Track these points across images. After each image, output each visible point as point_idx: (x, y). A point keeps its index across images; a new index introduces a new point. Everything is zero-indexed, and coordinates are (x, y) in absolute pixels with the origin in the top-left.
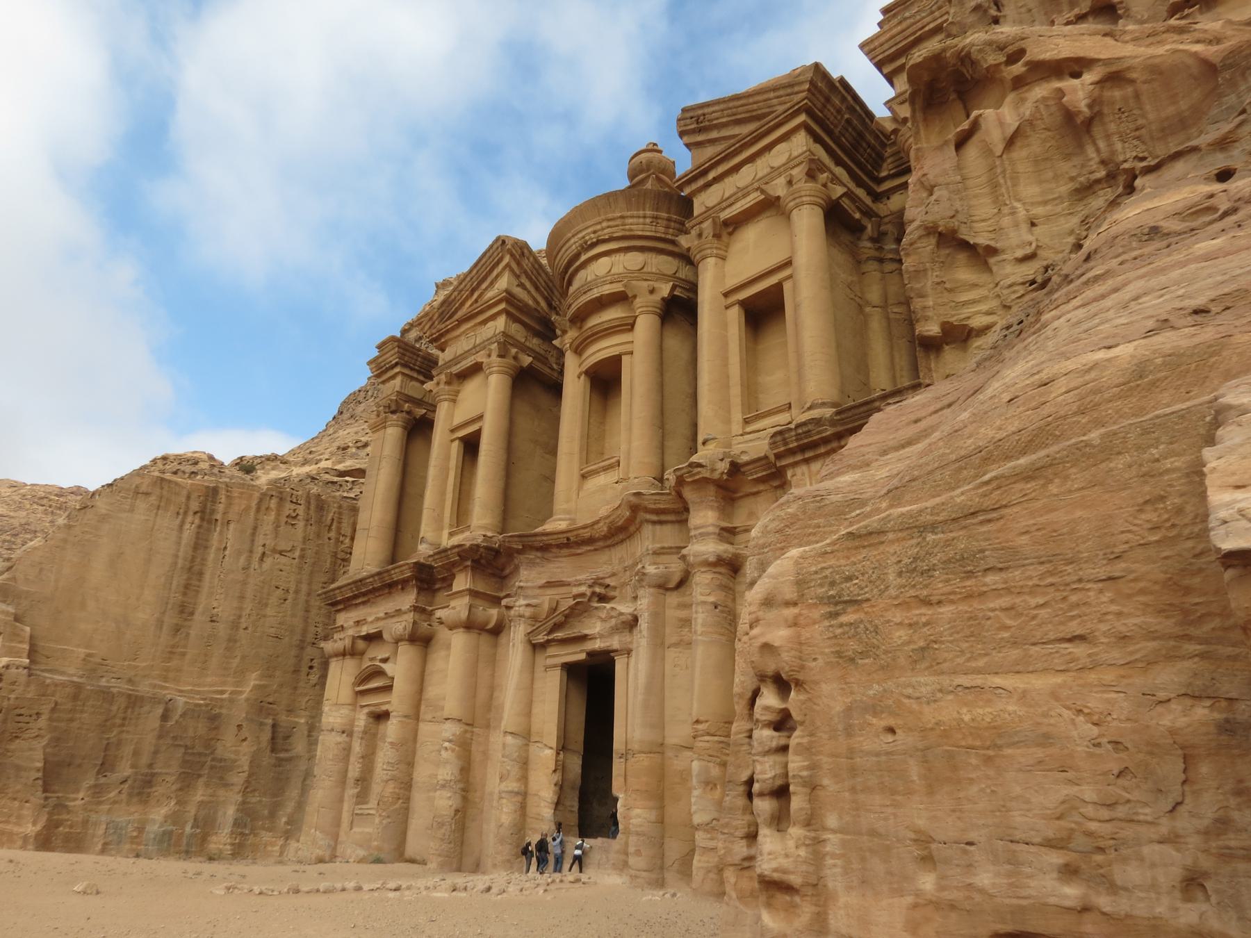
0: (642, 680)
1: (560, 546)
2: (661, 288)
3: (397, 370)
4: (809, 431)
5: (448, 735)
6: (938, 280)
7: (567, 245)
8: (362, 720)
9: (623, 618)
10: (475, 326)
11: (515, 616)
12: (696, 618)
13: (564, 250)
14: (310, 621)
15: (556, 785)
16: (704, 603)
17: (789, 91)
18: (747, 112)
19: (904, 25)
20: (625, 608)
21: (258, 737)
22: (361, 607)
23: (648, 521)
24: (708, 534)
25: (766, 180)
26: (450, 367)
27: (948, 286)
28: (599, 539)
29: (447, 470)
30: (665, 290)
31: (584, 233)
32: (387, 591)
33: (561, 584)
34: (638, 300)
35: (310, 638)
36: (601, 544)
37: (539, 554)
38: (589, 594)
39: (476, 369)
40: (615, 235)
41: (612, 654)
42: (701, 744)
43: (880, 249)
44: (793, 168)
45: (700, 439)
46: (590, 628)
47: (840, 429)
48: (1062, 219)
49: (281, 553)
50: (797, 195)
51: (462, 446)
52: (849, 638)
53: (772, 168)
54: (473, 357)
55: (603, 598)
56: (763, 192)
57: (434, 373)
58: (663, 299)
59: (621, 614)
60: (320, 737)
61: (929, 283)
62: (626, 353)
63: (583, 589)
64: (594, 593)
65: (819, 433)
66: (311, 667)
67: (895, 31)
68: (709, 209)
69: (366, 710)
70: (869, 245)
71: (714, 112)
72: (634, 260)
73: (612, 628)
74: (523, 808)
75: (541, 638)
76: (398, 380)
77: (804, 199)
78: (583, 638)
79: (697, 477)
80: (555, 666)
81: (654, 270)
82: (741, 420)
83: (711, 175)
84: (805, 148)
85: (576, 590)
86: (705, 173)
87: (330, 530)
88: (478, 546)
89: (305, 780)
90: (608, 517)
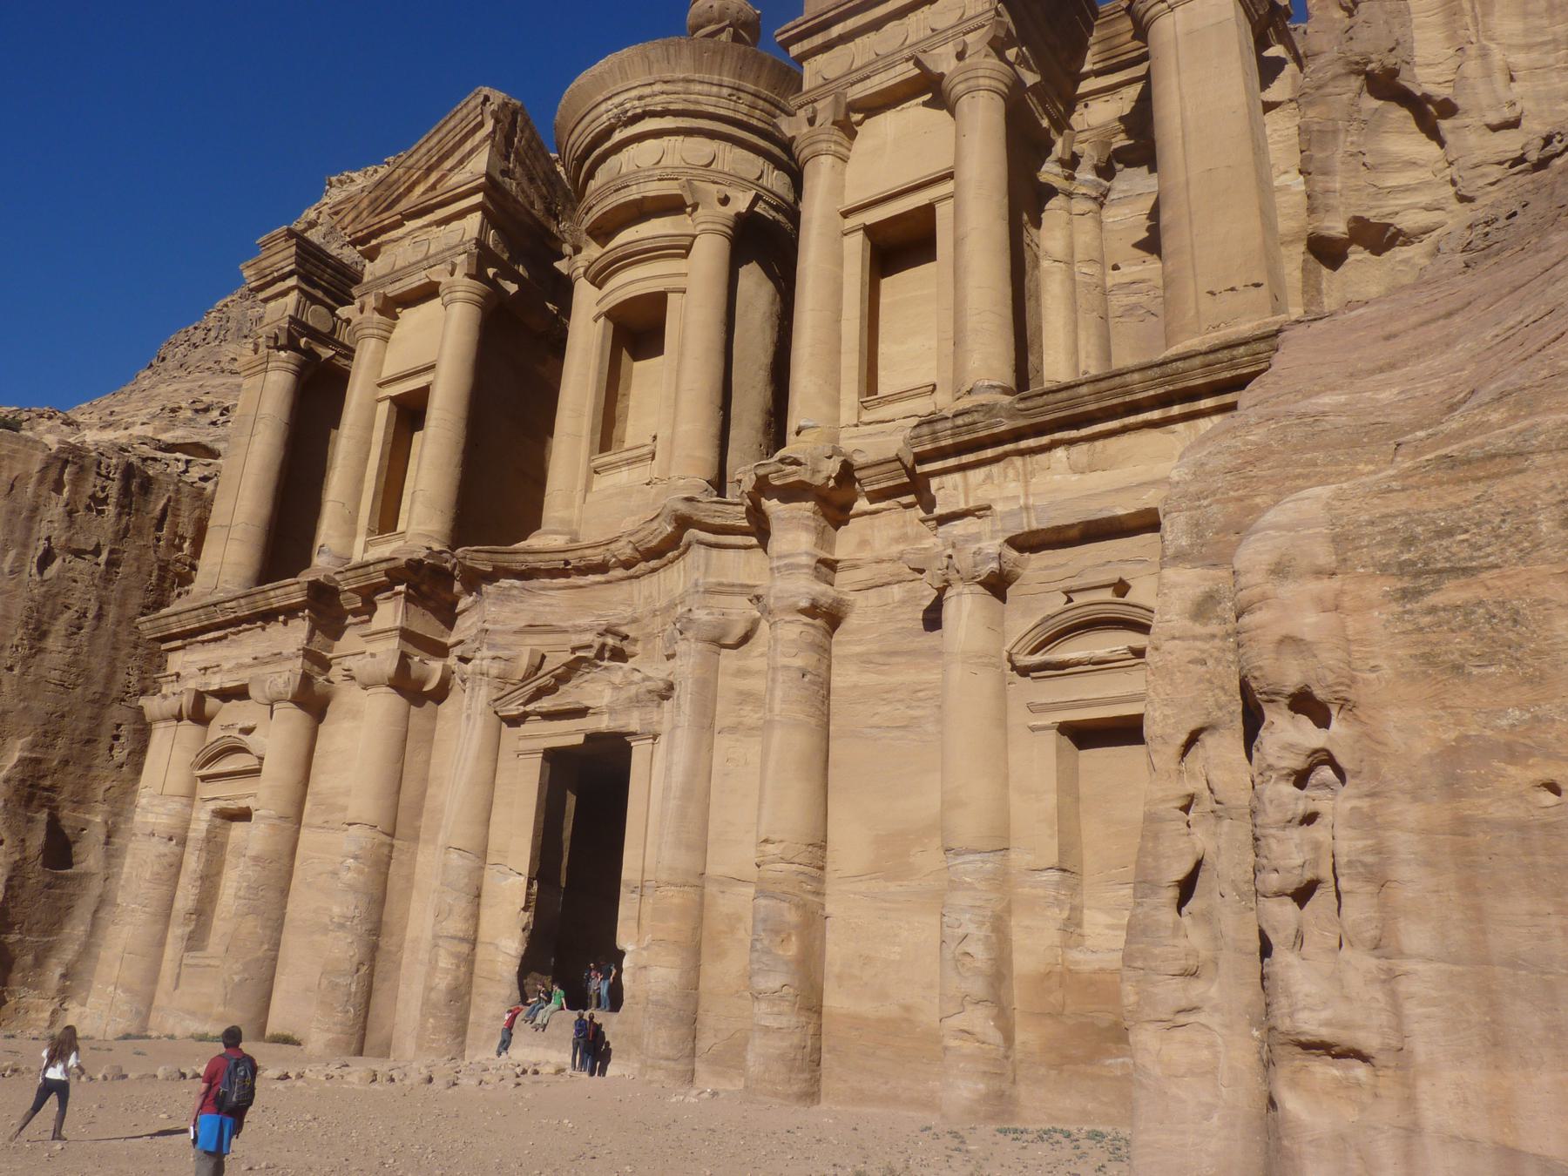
0: (678, 776)
1: (553, 573)
2: (737, 198)
3: (292, 281)
4: (974, 423)
5: (353, 848)
6: (1354, 149)
8: (202, 820)
9: (650, 685)
14: (119, 664)
15: (524, 930)
20: (658, 672)
21: (23, 840)
22: (212, 645)
23: (701, 543)
24: (799, 566)
25: (923, 46)
26: (383, 285)
27: (1368, 159)
29: (368, 443)
30: (741, 202)
33: (550, 629)
35: (115, 691)
38: (597, 646)
39: (428, 292)
40: (672, 107)
41: (628, 739)
43: (1071, 178)
44: (968, 32)
45: (792, 426)
47: (1021, 423)
48: (1554, 74)
49: (78, 553)
50: (969, 75)
51: (395, 409)
52: (1453, 631)
53: (933, 30)
54: (424, 273)
55: (619, 655)
56: (918, 63)
57: (355, 291)
58: (738, 215)
59: (647, 679)
60: (131, 845)
61: (1339, 155)
63: (587, 638)
64: (603, 646)
65: (988, 427)
66: (116, 738)
68: (827, 81)
69: (212, 806)
70: (1057, 169)
72: (701, 149)
73: (630, 700)
74: (469, 961)
75: (514, 709)
76: (294, 295)
77: (982, 81)
78: (581, 712)
79: (791, 480)
81: (726, 169)
82: (856, 404)
83: (836, 31)
84: (987, 6)
85: (576, 640)
87: (159, 527)
88: (420, 561)
89: (96, 911)
90: (631, 535)
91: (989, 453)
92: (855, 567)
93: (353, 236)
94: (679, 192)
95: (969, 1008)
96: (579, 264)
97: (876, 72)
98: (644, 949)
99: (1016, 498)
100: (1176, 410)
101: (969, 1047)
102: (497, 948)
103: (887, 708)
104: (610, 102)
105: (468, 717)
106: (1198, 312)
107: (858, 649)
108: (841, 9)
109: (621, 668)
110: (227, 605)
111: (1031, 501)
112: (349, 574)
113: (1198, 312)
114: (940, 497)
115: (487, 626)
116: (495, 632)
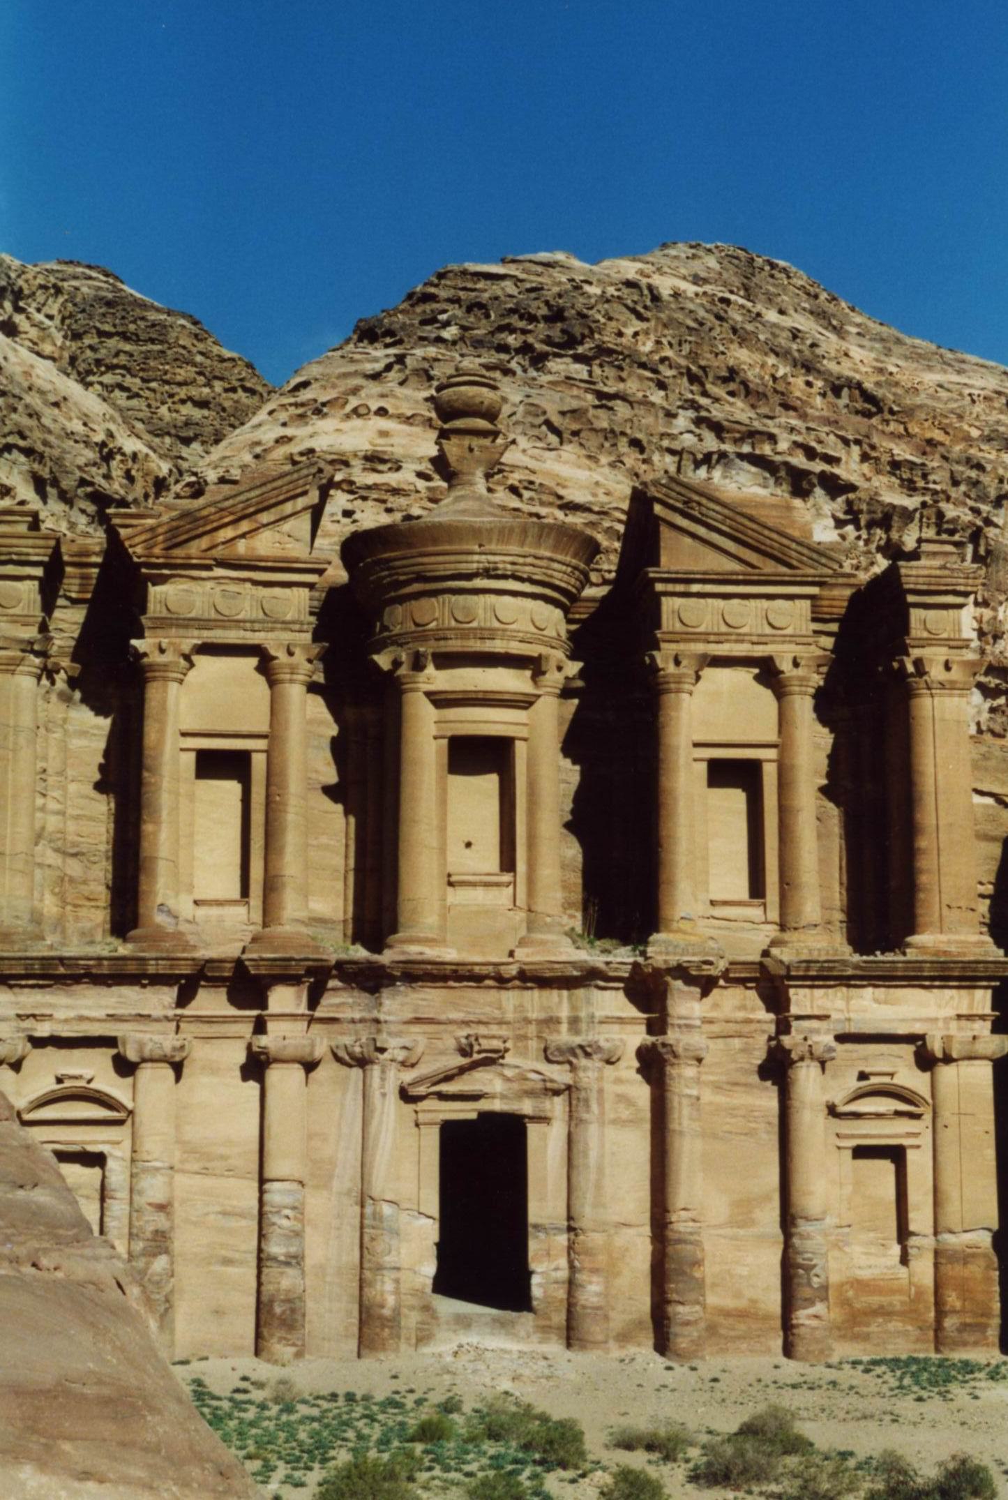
3: (39, 572)
9: (549, 1085)
12: (680, 1112)
13: (452, 558)
16: (690, 1096)
19: (947, 572)
22: (26, 990)
26: (186, 627)
31: (497, 558)
34: (547, 676)
46: (485, 1084)
47: (859, 973)
63: (496, 1044)
67: (938, 572)
75: (422, 1090)
79: (704, 973)
80: (435, 1124)
83: (695, 588)
85: (486, 1044)
90: (525, 964)
91: (832, 983)
93: (142, 560)
96: (421, 679)
97: (727, 641)
99: (842, 1011)
100: (937, 983)
103: (734, 1120)
105: (384, 1095)
106: (941, 915)
107: (711, 1078)
110: (82, 962)
111: (852, 1015)
113: (941, 915)
115: (388, 1018)
116: (391, 1022)
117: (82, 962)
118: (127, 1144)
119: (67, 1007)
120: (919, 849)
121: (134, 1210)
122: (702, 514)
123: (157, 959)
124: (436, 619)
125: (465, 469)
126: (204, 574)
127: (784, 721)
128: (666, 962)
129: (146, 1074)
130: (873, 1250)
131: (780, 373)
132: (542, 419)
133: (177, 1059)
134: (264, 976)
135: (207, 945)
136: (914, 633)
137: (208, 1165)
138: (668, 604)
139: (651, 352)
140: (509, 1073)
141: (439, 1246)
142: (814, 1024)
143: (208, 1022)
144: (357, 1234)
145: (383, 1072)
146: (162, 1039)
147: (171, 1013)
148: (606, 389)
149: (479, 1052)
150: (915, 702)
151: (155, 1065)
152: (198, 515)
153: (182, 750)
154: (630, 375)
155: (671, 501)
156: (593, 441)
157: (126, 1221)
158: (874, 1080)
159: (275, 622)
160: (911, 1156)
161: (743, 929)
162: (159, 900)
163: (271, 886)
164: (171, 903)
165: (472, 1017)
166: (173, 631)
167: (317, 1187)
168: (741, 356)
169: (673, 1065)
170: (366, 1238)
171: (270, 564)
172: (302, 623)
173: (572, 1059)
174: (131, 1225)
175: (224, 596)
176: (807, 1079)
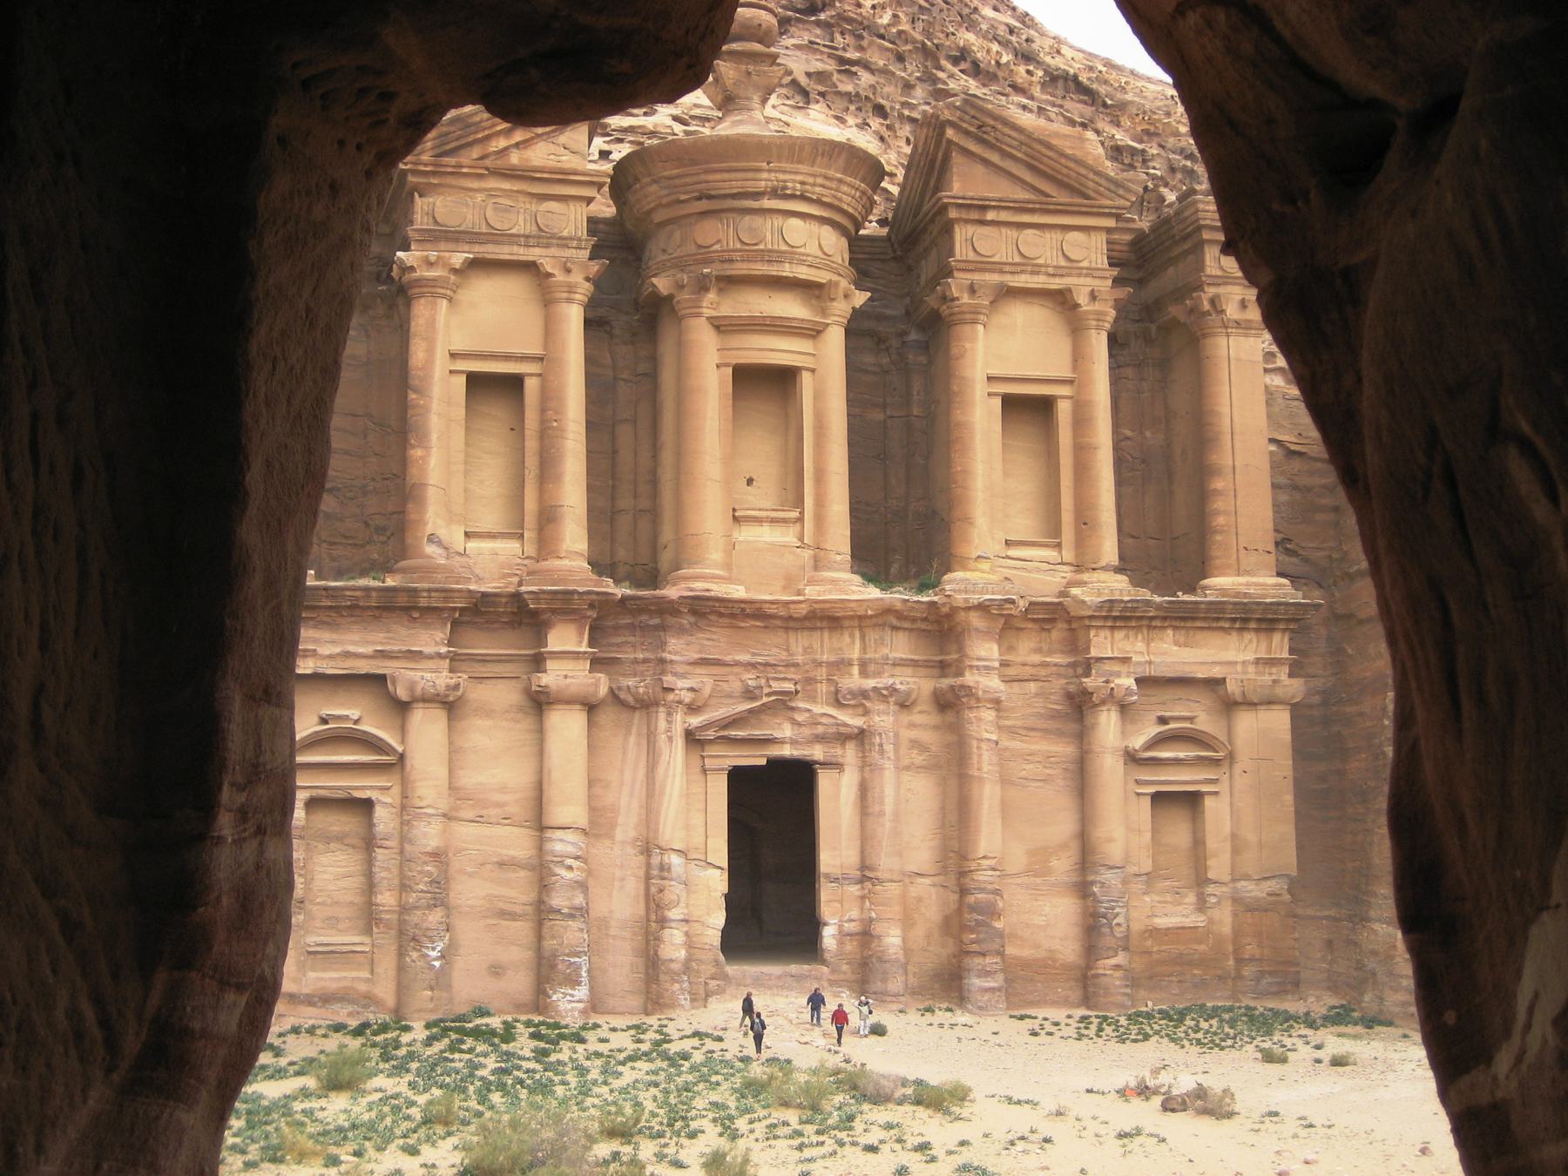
1: (721, 615)
7: (750, 175)
9: (842, 729)
10: (518, 192)
11: (673, 701)
12: (980, 756)
13: (739, 175)
16: (989, 740)
17: (1112, 187)
18: (1053, 169)
24: (994, 669)
26: (457, 240)
28: (781, 618)
30: (860, 298)
31: (787, 177)
32: (377, 613)
36: (778, 623)
37: (692, 619)
40: (824, 199)
42: (981, 878)
46: (773, 729)
47: (1162, 614)
50: (1102, 317)
62: (808, 369)
63: (789, 686)
71: (1009, 136)
75: (711, 734)
79: (1005, 612)
80: (722, 770)
83: (990, 216)
85: (776, 686)
86: (984, 208)
90: (817, 602)
92: (1008, 665)
94: (824, 281)
95: (1120, 953)
97: (1022, 272)
98: (846, 922)
101: (1118, 974)
102: (703, 924)
103: (1031, 766)
104: (773, 175)
105: (670, 739)
108: (1003, 204)
109: (809, 710)
110: (348, 593)
112: (542, 596)
114: (1094, 640)
115: (673, 658)
117: (348, 593)
118: (396, 790)
119: (333, 642)
120: (1215, 490)
121: (405, 859)
122: (997, 139)
123: (429, 590)
124: (719, 241)
125: (741, 95)
126: (475, 184)
127: (1079, 357)
128: (966, 600)
129: (418, 716)
130: (1169, 899)
131: (1004, 59)
132: (787, 79)
133: (451, 699)
134: (543, 611)
135: (479, 579)
136: (1208, 271)
137: (484, 812)
138: (961, 234)
139: (889, 25)
140: (800, 717)
141: (726, 896)
142: (1116, 668)
143: (479, 661)
144: (642, 887)
145: (669, 714)
146: (436, 678)
147: (444, 650)
148: (848, 55)
149: (769, 695)
150: (1208, 341)
151: (427, 705)
152: (470, 121)
153: (451, 372)
154: (871, 43)
155: (965, 125)
156: (840, 104)
157: (395, 871)
158: (1172, 726)
159: (550, 238)
160: (1209, 802)
161: (1039, 570)
162: (429, 529)
163: (548, 518)
164: (442, 533)
165: (759, 659)
166: (442, 246)
167: (597, 836)
168: (967, 37)
169: (970, 708)
170: (653, 890)
171: (545, 176)
172: (580, 240)
173: (864, 701)
174: (402, 876)
175: (495, 209)
176: (1108, 724)
